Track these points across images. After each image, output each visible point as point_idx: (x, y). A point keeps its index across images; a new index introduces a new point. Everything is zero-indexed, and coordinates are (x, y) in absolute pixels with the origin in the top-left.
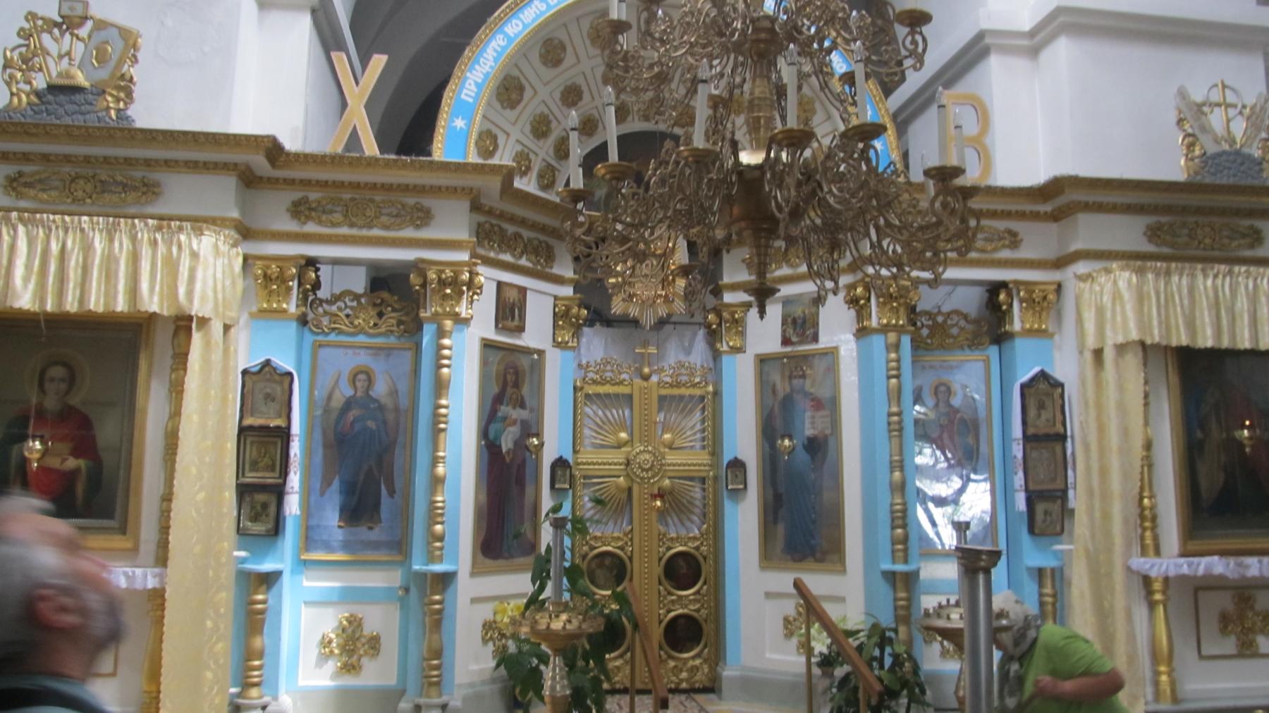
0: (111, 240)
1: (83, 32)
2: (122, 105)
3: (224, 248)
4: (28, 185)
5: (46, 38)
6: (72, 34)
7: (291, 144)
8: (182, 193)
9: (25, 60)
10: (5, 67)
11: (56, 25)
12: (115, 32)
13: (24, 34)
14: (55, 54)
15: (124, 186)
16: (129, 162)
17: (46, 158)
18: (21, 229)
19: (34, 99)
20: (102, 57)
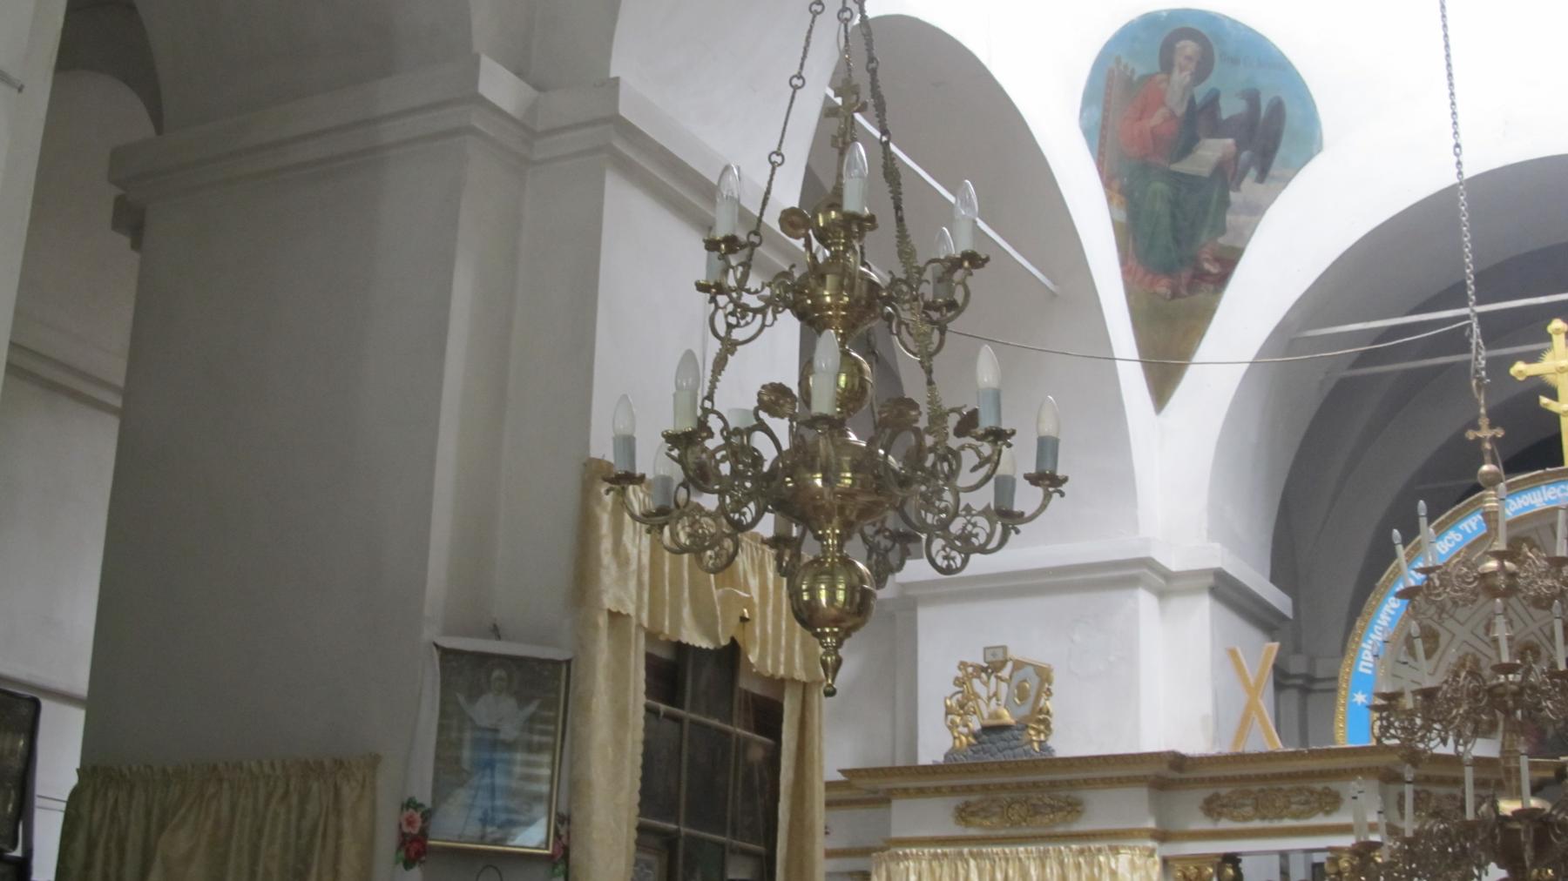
0: (1043, 866)
1: (1005, 673)
2: (1042, 737)
3: (1138, 862)
4: (973, 814)
5: (976, 682)
6: (998, 678)
7: (1195, 744)
8: (1103, 809)
9: (962, 706)
10: (947, 714)
11: (984, 670)
12: (1030, 670)
13: (959, 682)
14: (984, 694)
15: (1052, 807)
16: (1053, 784)
17: (985, 788)
18: (972, 863)
19: (972, 740)
20: (1022, 694)
